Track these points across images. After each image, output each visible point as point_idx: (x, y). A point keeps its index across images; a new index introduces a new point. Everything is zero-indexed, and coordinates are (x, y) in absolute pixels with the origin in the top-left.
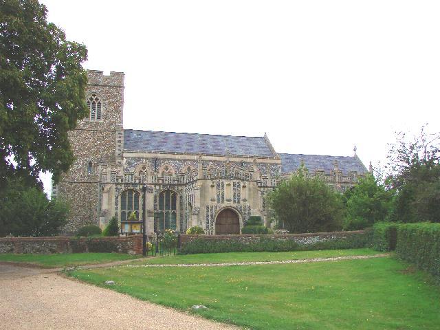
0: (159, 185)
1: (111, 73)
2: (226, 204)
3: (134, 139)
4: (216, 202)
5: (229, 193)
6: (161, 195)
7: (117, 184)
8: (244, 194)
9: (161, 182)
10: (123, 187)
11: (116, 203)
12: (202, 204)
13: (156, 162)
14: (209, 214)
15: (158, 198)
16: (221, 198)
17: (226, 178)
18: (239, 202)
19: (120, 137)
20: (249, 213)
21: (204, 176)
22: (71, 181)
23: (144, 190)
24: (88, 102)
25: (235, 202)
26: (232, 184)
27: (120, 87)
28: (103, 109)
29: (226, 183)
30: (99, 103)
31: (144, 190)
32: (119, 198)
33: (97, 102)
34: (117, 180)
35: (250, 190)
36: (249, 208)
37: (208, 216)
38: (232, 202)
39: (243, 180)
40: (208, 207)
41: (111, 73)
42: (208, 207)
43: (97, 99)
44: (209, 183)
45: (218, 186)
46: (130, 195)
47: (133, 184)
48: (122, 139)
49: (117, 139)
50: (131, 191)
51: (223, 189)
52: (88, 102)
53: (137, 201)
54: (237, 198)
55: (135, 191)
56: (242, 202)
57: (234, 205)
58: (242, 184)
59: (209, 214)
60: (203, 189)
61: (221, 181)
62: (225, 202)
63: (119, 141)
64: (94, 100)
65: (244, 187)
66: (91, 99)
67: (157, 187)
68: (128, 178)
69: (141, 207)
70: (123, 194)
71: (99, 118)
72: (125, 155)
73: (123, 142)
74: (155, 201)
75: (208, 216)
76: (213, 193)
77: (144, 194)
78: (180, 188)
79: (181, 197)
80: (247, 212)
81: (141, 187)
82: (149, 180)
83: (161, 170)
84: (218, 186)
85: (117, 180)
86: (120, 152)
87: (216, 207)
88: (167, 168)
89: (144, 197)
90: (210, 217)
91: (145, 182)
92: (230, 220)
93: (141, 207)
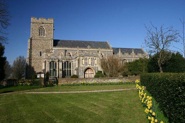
2: (88, 66)
5: (90, 62)
7: (48, 59)
9: (65, 58)
11: (48, 66)
14: (82, 70)
16: (86, 64)
17: (88, 56)
18: (93, 65)
23: (59, 61)
26: (90, 58)
30: (44, 30)
32: (49, 64)
34: (48, 58)
35: (97, 60)
43: (43, 28)
44: (82, 58)
45: (85, 59)
46: (52, 64)
54: (92, 64)
56: (94, 65)
59: (82, 70)
61: (86, 57)
62: (88, 65)
66: (41, 28)
67: (64, 60)
68: (52, 57)
69: (57, 68)
72: (54, 49)
75: (81, 71)
78: (72, 60)
79: (73, 64)
80: (96, 69)
81: (58, 60)
84: (85, 59)
85: (48, 58)
86: (52, 48)
87: (84, 67)
89: (59, 64)
90: (82, 71)
93: (57, 68)
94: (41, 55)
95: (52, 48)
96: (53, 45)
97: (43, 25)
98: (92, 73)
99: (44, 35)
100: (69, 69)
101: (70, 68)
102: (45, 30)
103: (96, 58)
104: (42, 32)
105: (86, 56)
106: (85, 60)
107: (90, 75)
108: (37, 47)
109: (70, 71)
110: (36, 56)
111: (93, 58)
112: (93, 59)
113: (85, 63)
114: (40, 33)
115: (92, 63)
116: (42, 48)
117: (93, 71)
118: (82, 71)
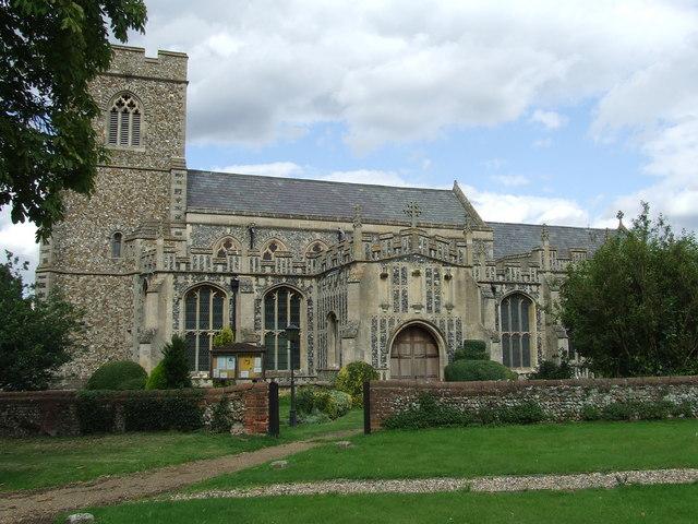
0: (265, 276)
1: (161, 53)
2: (411, 315)
3: (204, 189)
4: (391, 310)
5: (416, 290)
6: (269, 297)
7: (176, 274)
8: (448, 292)
10: (190, 281)
11: (175, 316)
12: (364, 315)
13: (252, 232)
15: (262, 305)
16: (401, 300)
17: (410, 258)
18: (437, 311)
23: (235, 286)
25: (429, 309)
27: (180, 82)
28: (143, 126)
30: (136, 113)
31: (235, 286)
32: (182, 304)
33: (131, 111)
34: (178, 264)
36: (459, 322)
37: (374, 341)
38: (424, 311)
39: (445, 264)
40: (374, 321)
41: (161, 53)
42: (374, 321)
43: (132, 105)
44: (377, 269)
45: (396, 275)
46: (204, 296)
47: (210, 274)
48: (184, 187)
49: (174, 187)
50: (205, 289)
51: (405, 283)
52: (114, 109)
53: (218, 309)
54: (433, 301)
55: (215, 290)
56: (444, 310)
57: (429, 317)
58: (443, 271)
60: (363, 282)
61: (402, 264)
62: (410, 310)
64: (126, 106)
65: (448, 278)
66: (120, 104)
67: (262, 281)
68: (202, 263)
70: (190, 296)
71: (136, 143)
72: (190, 218)
73: (184, 193)
74: (257, 311)
75: (374, 341)
76: (384, 290)
77: (234, 296)
79: (310, 302)
80: (454, 331)
81: (228, 279)
82: (243, 266)
83: (262, 247)
84: (396, 275)
85: (178, 264)
87: (392, 322)
89: (233, 301)
90: (379, 343)
91: (235, 271)
92: (419, 349)
94: (117, 252)
96: (183, 196)
97: (133, 86)
100: (522, 334)
101: (526, 327)
102: (141, 111)
103: (453, 271)
104: (125, 126)
105: (400, 258)
109: (527, 338)
110: (88, 255)
112: (437, 276)
113: (396, 298)
114: (113, 128)
115: (429, 298)
117: (434, 341)
118: (382, 340)
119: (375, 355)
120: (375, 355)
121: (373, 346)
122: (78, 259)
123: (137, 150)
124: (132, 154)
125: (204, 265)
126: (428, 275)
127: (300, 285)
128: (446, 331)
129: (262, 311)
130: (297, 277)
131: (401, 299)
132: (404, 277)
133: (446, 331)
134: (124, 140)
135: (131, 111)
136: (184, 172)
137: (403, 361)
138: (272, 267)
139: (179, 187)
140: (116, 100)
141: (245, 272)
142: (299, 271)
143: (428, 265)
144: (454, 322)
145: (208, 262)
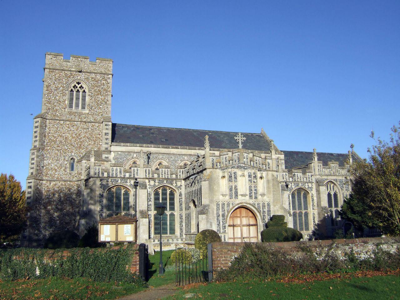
0: (154, 179)
2: (241, 200)
4: (227, 198)
5: (243, 185)
8: (261, 186)
12: (211, 201)
14: (221, 213)
16: (234, 192)
18: (256, 198)
19: (107, 129)
20: (269, 211)
21: (213, 164)
22: (50, 178)
23: (136, 185)
24: (72, 90)
25: (251, 197)
28: (87, 98)
29: (239, 172)
30: (84, 91)
33: (81, 91)
35: (268, 181)
36: (269, 205)
37: (218, 216)
38: (248, 197)
39: (260, 170)
40: (218, 205)
42: (218, 205)
43: (81, 87)
44: (219, 173)
49: (104, 131)
51: (236, 181)
52: (72, 90)
54: (253, 193)
56: (259, 197)
57: (251, 201)
58: (259, 174)
59: (221, 213)
60: (210, 179)
62: (239, 197)
63: (106, 134)
64: (78, 88)
65: (261, 178)
67: (152, 183)
71: (83, 108)
72: (113, 148)
74: (149, 200)
75: (218, 216)
76: (223, 185)
77: (136, 192)
79: (180, 195)
80: (266, 210)
81: (132, 182)
82: (141, 174)
84: (230, 177)
86: (106, 146)
87: (228, 205)
88: (160, 164)
89: (135, 195)
91: (136, 177)
92: (245, 221)
94: (72, 168)
95: (106, 146)
96: (110, 136)
97: (82, 76)
98: (251, 223)
99: (83, 108)
100: (304, 212)
101: (306, 208)
102: (87, 91)
103: (264, 174)
104: (78, 99)
106: (230, 180)
107: (245, 229)
108: (61, 142)
109: (306, 215)
111: (253, 175)
112: (255, 177)
113: (231, 190)
114: (71, 100)
116: (77, 148)
118: (223, 216)
119: (219, 225)
120: (219, 225)
121: (218, 219)
122: (50, 172)
123: (84, 112)
124: (80, 114)
125: (118, 174)
126: (250, 176)
127: (174, 185)
128: (261, 210)
129: (153, 200)
130: (172, 180)
131: (234, 191)
132: (236, 178)
133: (261, 210)
134: (77, 106)
135: (81, 91)
136: (110, 124)
137: (235, 228)
138: (158, 174)
139: (107, 131)
140: (73, 85)
141: (142, 177)
142: (174, 176)
143: (250, 171)
144: (266, 205)
145: (120, 172)
